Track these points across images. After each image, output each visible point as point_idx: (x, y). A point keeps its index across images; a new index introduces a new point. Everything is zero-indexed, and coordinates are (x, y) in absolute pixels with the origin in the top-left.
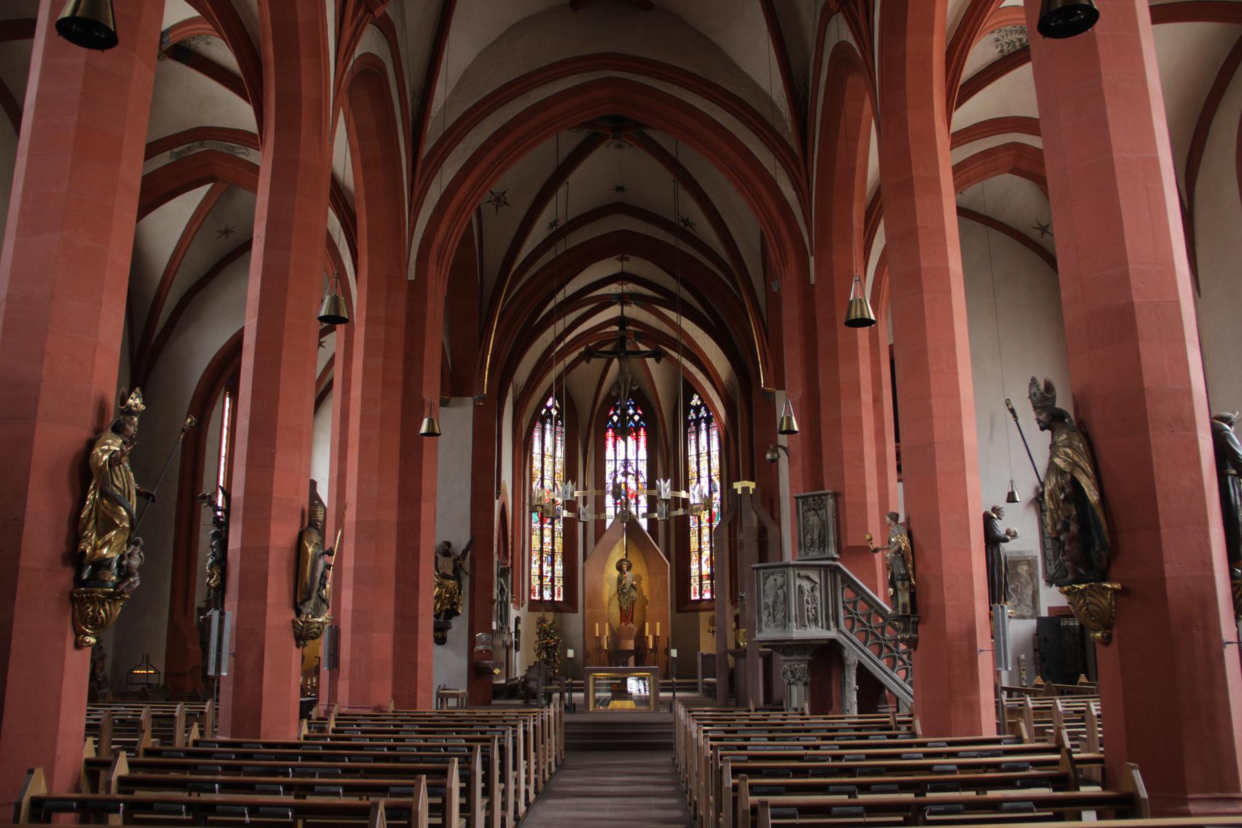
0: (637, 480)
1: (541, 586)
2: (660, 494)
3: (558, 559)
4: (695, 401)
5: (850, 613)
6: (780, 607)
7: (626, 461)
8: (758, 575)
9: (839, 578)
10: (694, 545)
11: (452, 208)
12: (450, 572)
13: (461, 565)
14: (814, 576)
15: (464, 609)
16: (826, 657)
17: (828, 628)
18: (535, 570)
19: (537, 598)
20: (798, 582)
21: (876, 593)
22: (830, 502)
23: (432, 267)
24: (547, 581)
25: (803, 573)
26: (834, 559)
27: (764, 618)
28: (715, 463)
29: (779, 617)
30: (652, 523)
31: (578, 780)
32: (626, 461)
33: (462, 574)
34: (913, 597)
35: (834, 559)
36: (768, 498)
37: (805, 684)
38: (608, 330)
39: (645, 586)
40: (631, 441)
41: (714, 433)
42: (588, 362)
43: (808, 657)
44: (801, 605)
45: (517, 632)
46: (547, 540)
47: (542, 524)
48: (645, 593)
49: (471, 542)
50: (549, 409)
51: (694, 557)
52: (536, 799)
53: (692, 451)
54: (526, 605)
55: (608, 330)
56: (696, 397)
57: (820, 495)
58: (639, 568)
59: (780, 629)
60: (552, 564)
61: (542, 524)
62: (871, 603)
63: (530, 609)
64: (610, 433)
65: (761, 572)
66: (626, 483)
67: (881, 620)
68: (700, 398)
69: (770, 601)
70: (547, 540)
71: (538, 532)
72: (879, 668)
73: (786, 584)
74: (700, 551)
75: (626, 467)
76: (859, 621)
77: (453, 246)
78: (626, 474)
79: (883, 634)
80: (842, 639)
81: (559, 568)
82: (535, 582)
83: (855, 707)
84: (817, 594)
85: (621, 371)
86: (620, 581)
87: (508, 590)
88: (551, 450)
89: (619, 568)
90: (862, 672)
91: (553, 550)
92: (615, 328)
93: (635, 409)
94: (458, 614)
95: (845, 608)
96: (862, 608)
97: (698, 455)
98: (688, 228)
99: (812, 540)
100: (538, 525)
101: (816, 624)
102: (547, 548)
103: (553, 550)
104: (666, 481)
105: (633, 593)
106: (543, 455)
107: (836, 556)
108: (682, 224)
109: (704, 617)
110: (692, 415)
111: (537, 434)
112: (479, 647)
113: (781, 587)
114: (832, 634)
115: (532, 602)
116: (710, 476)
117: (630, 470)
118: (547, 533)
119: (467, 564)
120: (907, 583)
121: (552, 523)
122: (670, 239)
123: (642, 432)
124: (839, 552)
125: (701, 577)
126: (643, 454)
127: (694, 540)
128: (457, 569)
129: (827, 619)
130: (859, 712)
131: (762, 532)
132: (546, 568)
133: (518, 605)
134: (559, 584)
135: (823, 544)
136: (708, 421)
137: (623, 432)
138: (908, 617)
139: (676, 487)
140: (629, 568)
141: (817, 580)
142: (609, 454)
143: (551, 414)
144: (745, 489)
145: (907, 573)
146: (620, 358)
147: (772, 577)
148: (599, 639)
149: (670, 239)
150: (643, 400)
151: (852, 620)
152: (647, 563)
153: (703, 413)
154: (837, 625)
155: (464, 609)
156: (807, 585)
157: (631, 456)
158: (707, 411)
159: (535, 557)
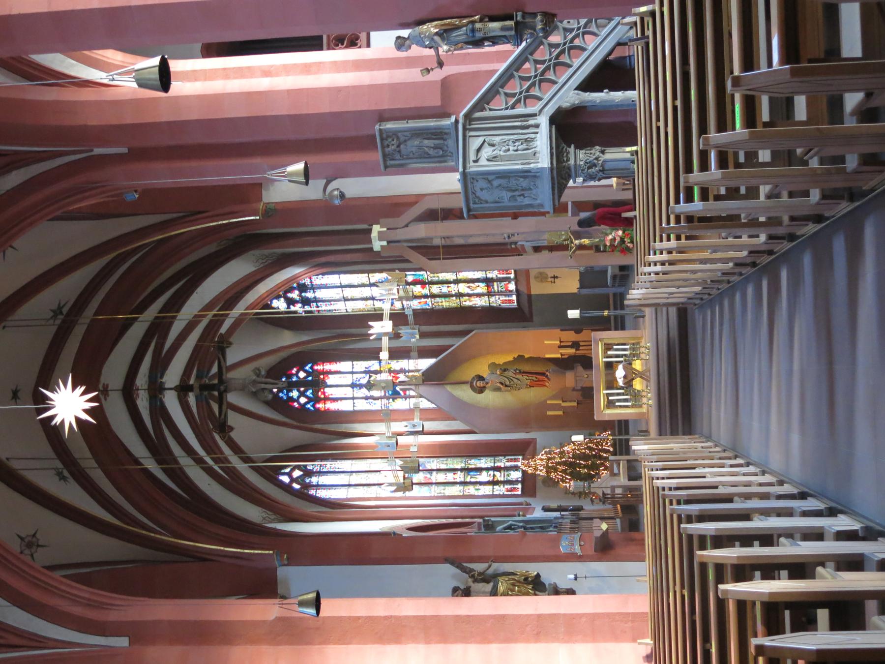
0: (376, 372)
2: (386, 334)
3: (474, 463)
4: (280, 305)
5: (519, 101)
6: (513, 183)
7: (353, 386)
8: (475, 210)
9: (478, 115)
10: (452, 303)
11: (36, 595)
12: (489, 587)
13: (480, 574)
14: (475, 144)
15: (533, 569)
16: (570, 127)
17: (537, 126)
18: (487, 490)
19: (519, 486)
20: (483, 161)
21: (496, 71)
22: (390, 125)
23: (113, 616)
24: (499, 476)
25: (472, 156)
26: (457, 121)
27: (527, 201)
29: (524, 183)
30: (424, 353)
31: (722, 414)
32: (353, 386)
33: (490, 571)
34: (493, 19)
35: (457, 121)
36: (391, 208)
37: (603, 152)
38: (194, 410)
39: (501, 360)
41: (318, 280)
42: (231, 429)
43: (572, 149)
44: (510, 158)
45: (560, 509)
49: (452, 563)
50: (293, 480)
52: (741, 457)
53: (341, 308)
55: (194, 410)
56: (275, 303)
57: (382, 139)
58: (482, 367)
59: (538, 182)
60: (480, 470)
62: (507, 76)
64: (320, 406)
65: (472, 205)
67: (527, 65)
68: (278, 297)
69: (506, 195)
70: (450, 477)
72: (584, 66)
73: (486, 176)
74: (460, 295)
75: (361, 386)
76: (528, 90)
77: (85, 592)
78: (369, 386)
79: (543, 62)
80: (550, 110)
81: (484, 463)
82: (500, 490)
83: (630, 94)
84: (497, 139)
85: (243, 389)
86: (498, 389)
87: (510, 521)
89: (481, 390)
90: (587, 85)
91: (462, 470)
92: (192, 399)
94: (538, 576)
95: (513, 107)
96: (515, 87)
98: (65, 310)
99: (435, 148)
101: (532, 140)
102: (460, 477)
103: (462, 470)
104: (371, 327)
107: (453, 119)
108: (58, 322)
109: (537, 289)
110: (298, 308)
111: (322, 494)
112: (577, 549)
113: (489, 182)
114: (543, 121)
115: (524, 493)
116: (371, 285)
117: (364, 381)
119: (479, 567)
120: (478, 25)
122: (79, 331)
123: (319, 367)
124: (448, 116)
125: (489, 294)
126: (345, 366)
127: (445, 303)
128: (484, 578)
129: (527, 127)
130: (634, 89)
131: (431, 215)
132: (484, 477)
133: (528, 508)
134: (502, 462)
135: (439, 134)
138: (517, 23)
139: (378, 317)
140: (481, 378)
141: (481, 140)
144: (381, 236)
145: (466, 25)
146: (226, 391)
147: (479, 193)
148: (566, 411)
149: (79, 331)
150: (280, 370)
151: (527, 97)
152: (474, 357)
153: (295, 295)
154: (534, 115)
155: (533, 569)
156: (487, 152)
157: (348, 379)
158: (291, 290)
159: (471, 490)
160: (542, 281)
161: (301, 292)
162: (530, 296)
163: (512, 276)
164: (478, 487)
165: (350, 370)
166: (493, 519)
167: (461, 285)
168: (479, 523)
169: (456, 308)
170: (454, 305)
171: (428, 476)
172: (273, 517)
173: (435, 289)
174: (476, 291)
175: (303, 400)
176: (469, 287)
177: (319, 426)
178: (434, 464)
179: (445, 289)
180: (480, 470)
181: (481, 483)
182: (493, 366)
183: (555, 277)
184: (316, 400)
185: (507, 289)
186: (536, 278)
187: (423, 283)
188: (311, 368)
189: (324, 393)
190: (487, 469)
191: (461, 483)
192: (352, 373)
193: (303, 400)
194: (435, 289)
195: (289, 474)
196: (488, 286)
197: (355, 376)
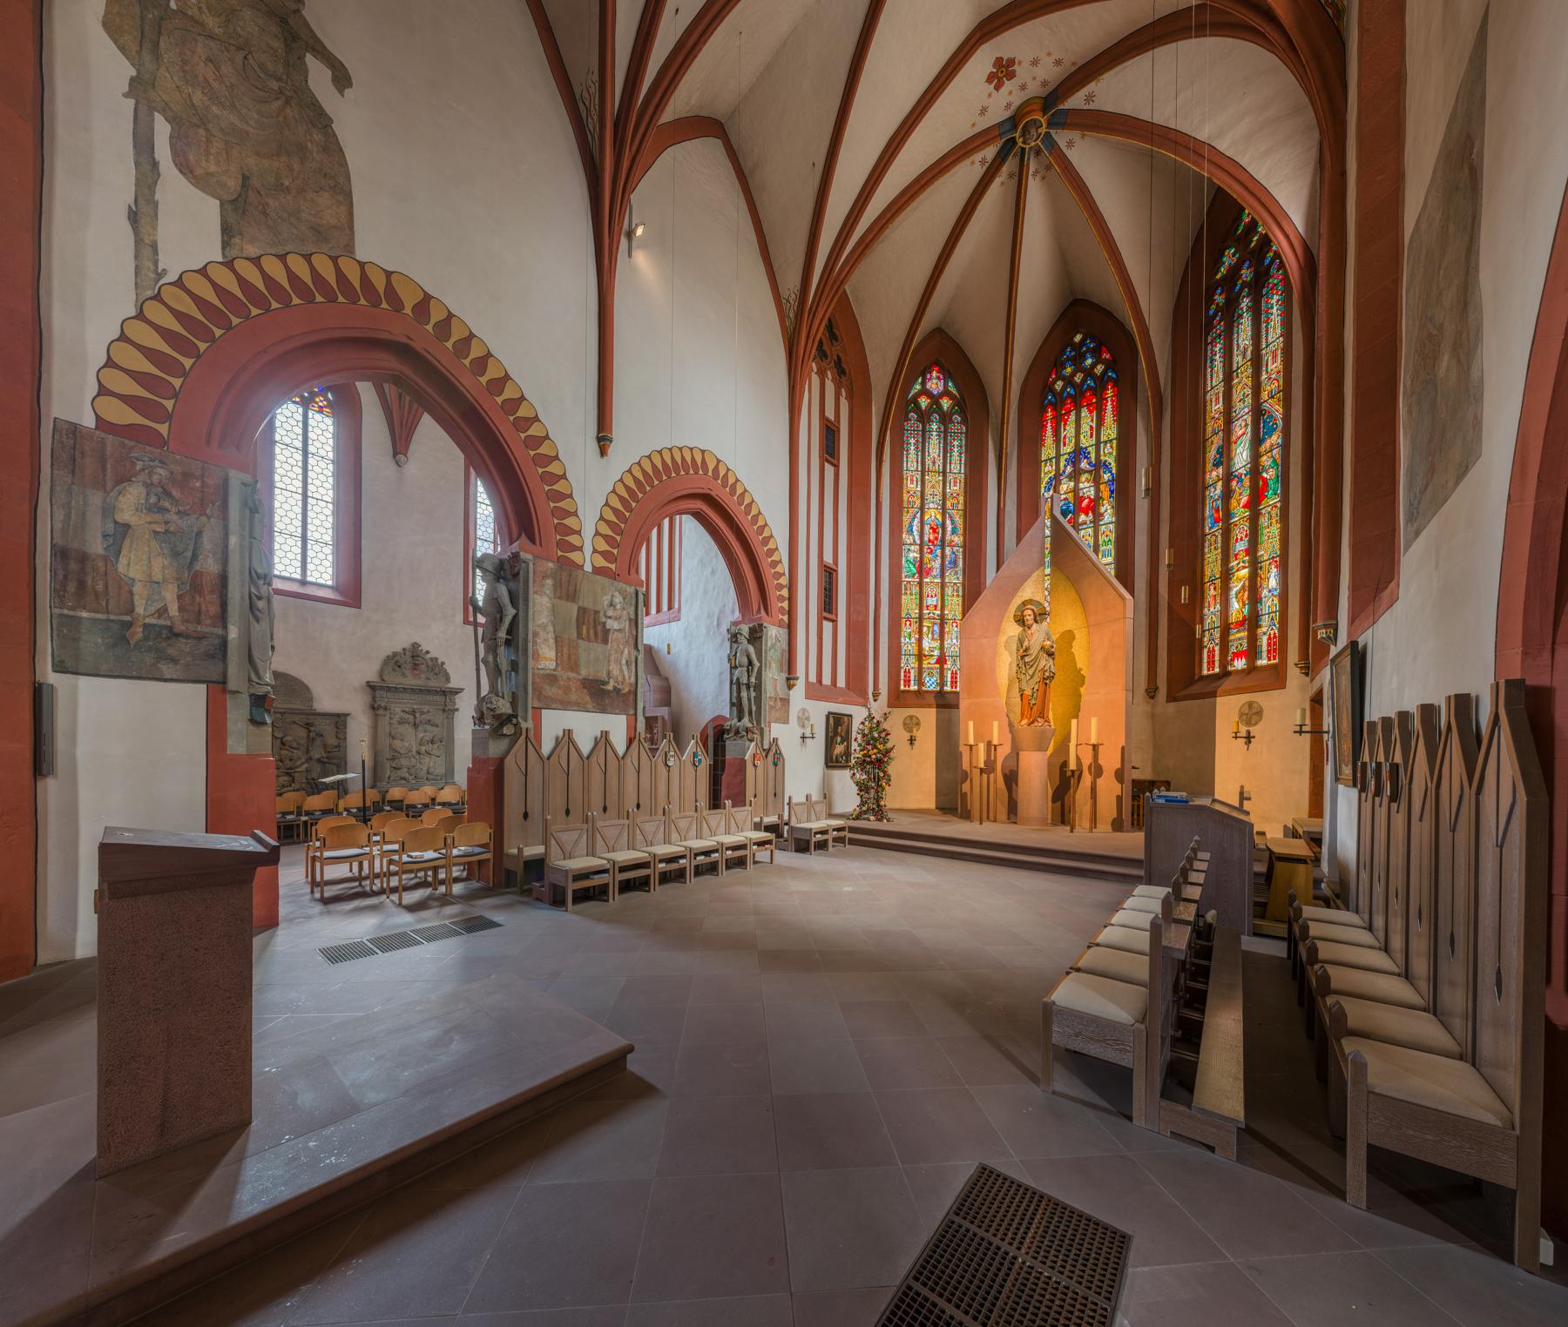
10: (1212, 567)
32: (1079, 453)
39: (1079, 650)
40: (1087, 419)
48: (1081, 662)
50: (935, 400)
51: (1211, 592)
66: (1076, 490)
74: (1226, 576)
86: (1021, 642)
89: (1021, 621)
93: (1096, 353)
105: (1044, 662)
123: (1110, 393)
125: (1226, 629)
126: (1110, 430)
127: (1212, 557)
142: (1048, 451)
143: (940, 406)
152: (1084, 604)
160: (1241, 715)
162: (1214, 695)
170: (1208, 572)
182: (1069, 636)
183: (1249, 738)
186: (1250, 705)
193: (1059, 385)
195: (946, 393)
197: (1092, 450)
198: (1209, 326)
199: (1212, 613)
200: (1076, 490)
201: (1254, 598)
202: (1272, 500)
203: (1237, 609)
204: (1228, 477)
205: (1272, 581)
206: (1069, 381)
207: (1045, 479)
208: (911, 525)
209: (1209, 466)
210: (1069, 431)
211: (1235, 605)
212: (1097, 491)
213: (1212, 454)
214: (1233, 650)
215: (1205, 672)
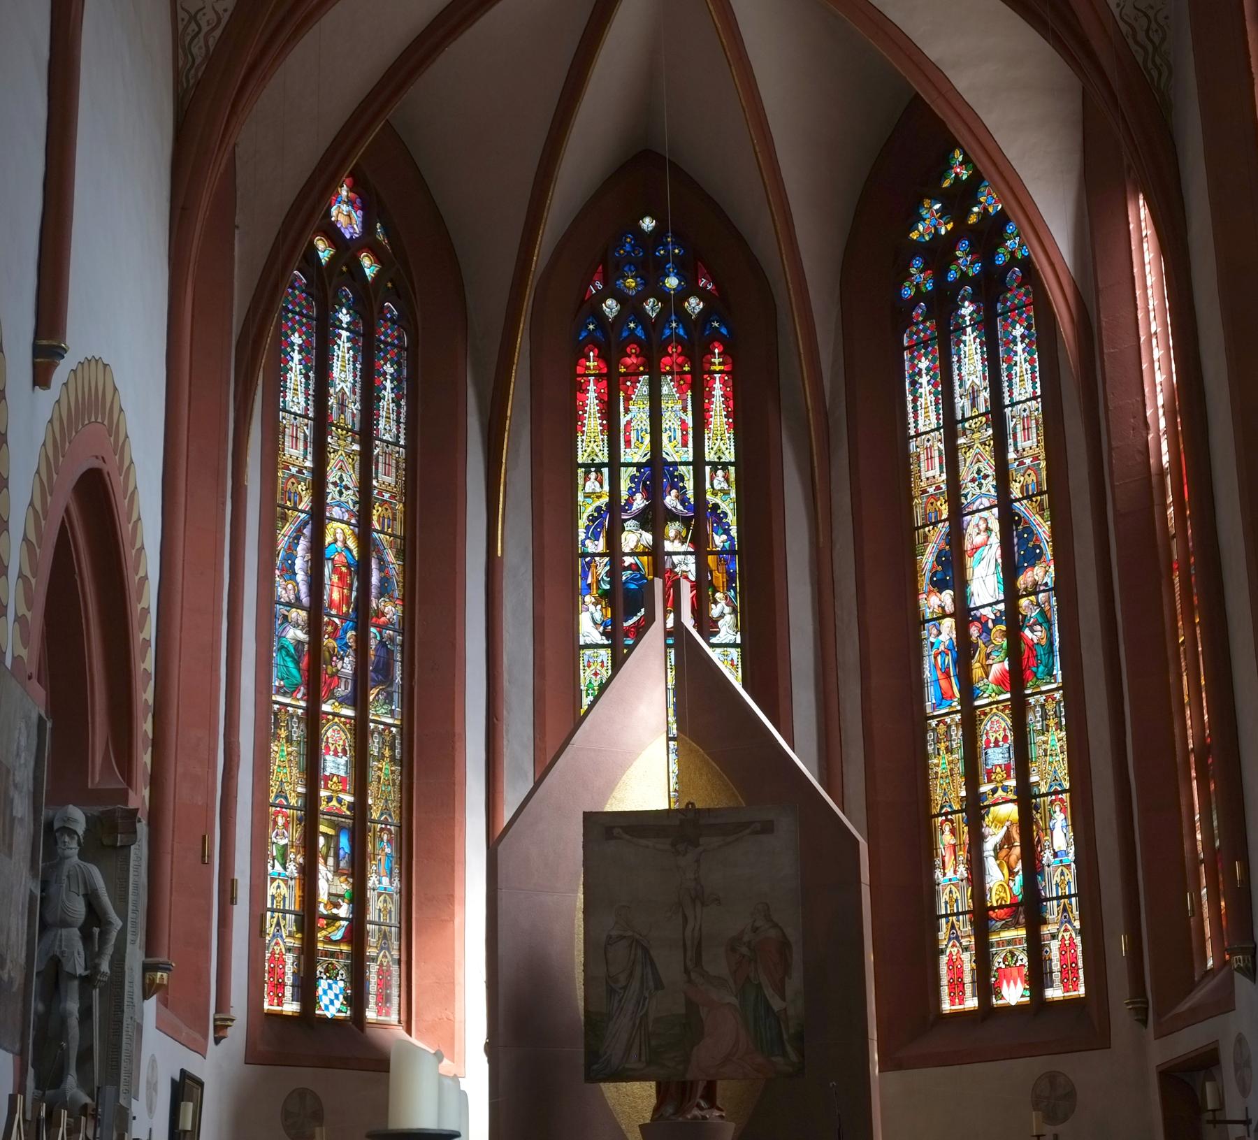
1: (308, 954)
7: (656, 473)
10: (947, 786)
18: (282, 890)
19: (291, 1007)
28: (1027, 443)
46: (335, 765)
47: (314, 700)
53: (924, 415)
54: (237, 1033)
60: (357, 871)
61: (314, 700)
63: (253, 1056)
66: (655, 552)
70: (335, 765)
71: (298, 732)
74: (975, 809)
75: (654, 492)
82: (283, 941)
88: (354, 408)
91: (360, 808)
97: (951, 426)
100: (299, 703)
102: (336, 798)
103: (360, 808)
106: (321, 423)
116: (1004, 503)
118: (335, 736)
121: (359, 700)
125: (982, 917)
126: (721, 443)
127: (945, 764)
133: (195, 1019)
136: (989, 289)
137: (639, 351)
142: (591, 442)
150: (711, 239)
153: (965, 262)
157: (676, 451)
159: (284, 836)
161: (973, 281)
163: (1054, 993)
164: (296, 859)
165: (710, 456)
166: (139, 852)
167: (1010, 811)
168: (124, 796)
169: (927, 800)
170: (938, 796)
171: (343, 690)
172: (198, 50)
173: (997, 726)
174: (991, 865)
175: (611, 307)
176: (1008, 838)
177: (522, 341)
178: (384, 715)
179: (997, 757)
180: (357, 871)
181: (308, 876)
184: (609, 357)
185: (1004, 975)
186: (1052, 1077)
187: (1016, 679)
188: (716, 336)
189: (634, 375)
190: (359, 900)
191: (311, 799)
192: (698, 463)
193: (611, 307)
194: (997, 726)
195: (367, 242)
196: (1014, 906)
198: (901, 316)
199: (950, 876)
200: (655, 552)
201: (1032, 867)
202: (1047, 688)
203: (1001, 882)
204: (963, 614)
205: (1060, 836)
206: (632, 307)
207: (587, 509)
208: (291, 556)
209: (924, 583)
210: (636, 415)
211: (995, 875)
212: (701, 566)
213: (927, 560)
214: (998, 962)
215: (946, 1007)
